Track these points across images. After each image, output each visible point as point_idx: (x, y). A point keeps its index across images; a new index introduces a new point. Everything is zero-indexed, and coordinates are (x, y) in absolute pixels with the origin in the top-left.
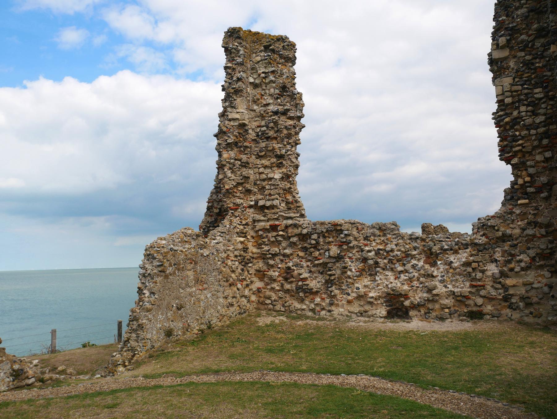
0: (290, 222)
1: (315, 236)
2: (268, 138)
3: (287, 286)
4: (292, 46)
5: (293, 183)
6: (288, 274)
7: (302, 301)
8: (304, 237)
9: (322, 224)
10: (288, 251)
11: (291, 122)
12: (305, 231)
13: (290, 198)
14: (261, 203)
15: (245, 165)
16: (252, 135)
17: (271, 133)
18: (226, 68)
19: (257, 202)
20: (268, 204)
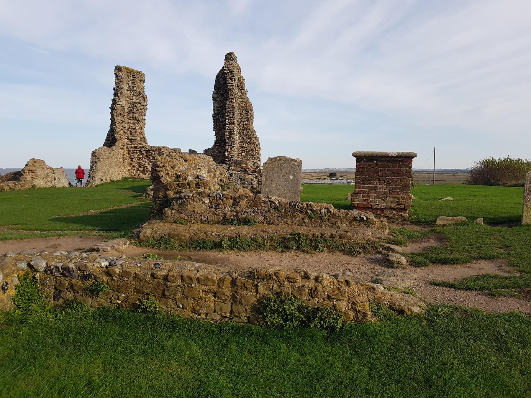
0: (142, 146)
1: (151, 151)
2: (134, 113)
3: (141, 169)
4: (143, 75)
5: (143, 131)
6: (140, 165)
7: (146, 174)
8: (148, 152)
9: (154, 147)
10: (141, 156)
11: (142, 107)
12: (147, 149)
13: (142, 137)
14: (130, 138)
15: (123, 122)
16: (126, 110)
17: (135, 110)
18: (116, 82)
19: (128, 138)
20: (133, 138)
